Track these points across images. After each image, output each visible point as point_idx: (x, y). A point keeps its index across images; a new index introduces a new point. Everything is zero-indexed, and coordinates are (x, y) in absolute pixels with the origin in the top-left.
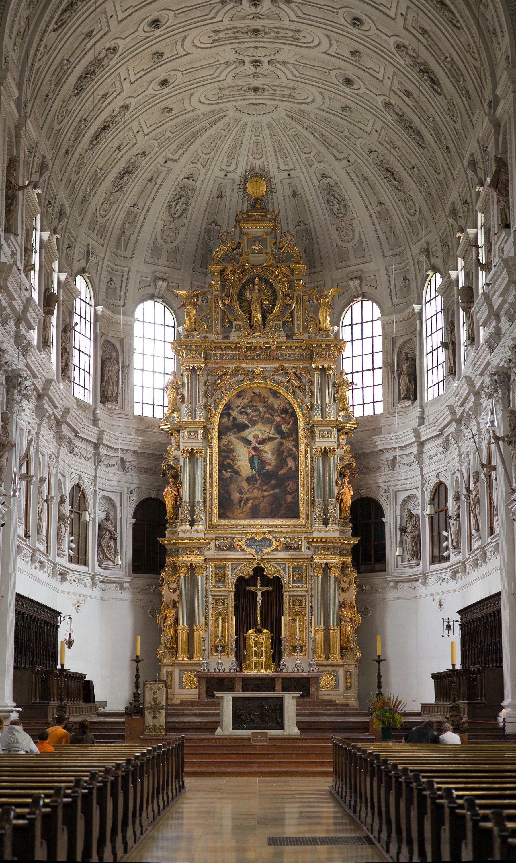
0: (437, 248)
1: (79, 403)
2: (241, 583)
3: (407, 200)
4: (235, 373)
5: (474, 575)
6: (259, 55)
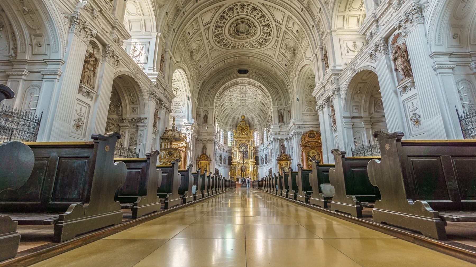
0: (265, 125)
1: (221, 145)
2: (242, 167)
3: (262, 119)
4: (240, 140)
5: (270, 165)
6: (243, 102)
